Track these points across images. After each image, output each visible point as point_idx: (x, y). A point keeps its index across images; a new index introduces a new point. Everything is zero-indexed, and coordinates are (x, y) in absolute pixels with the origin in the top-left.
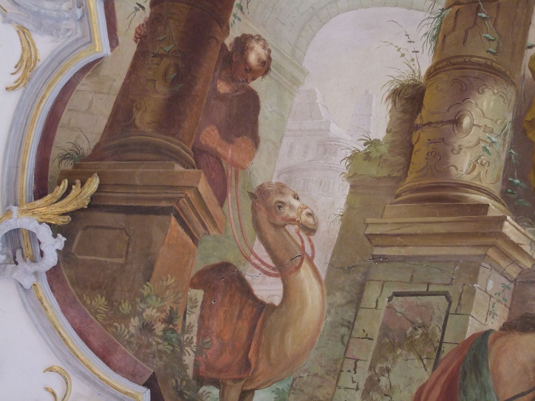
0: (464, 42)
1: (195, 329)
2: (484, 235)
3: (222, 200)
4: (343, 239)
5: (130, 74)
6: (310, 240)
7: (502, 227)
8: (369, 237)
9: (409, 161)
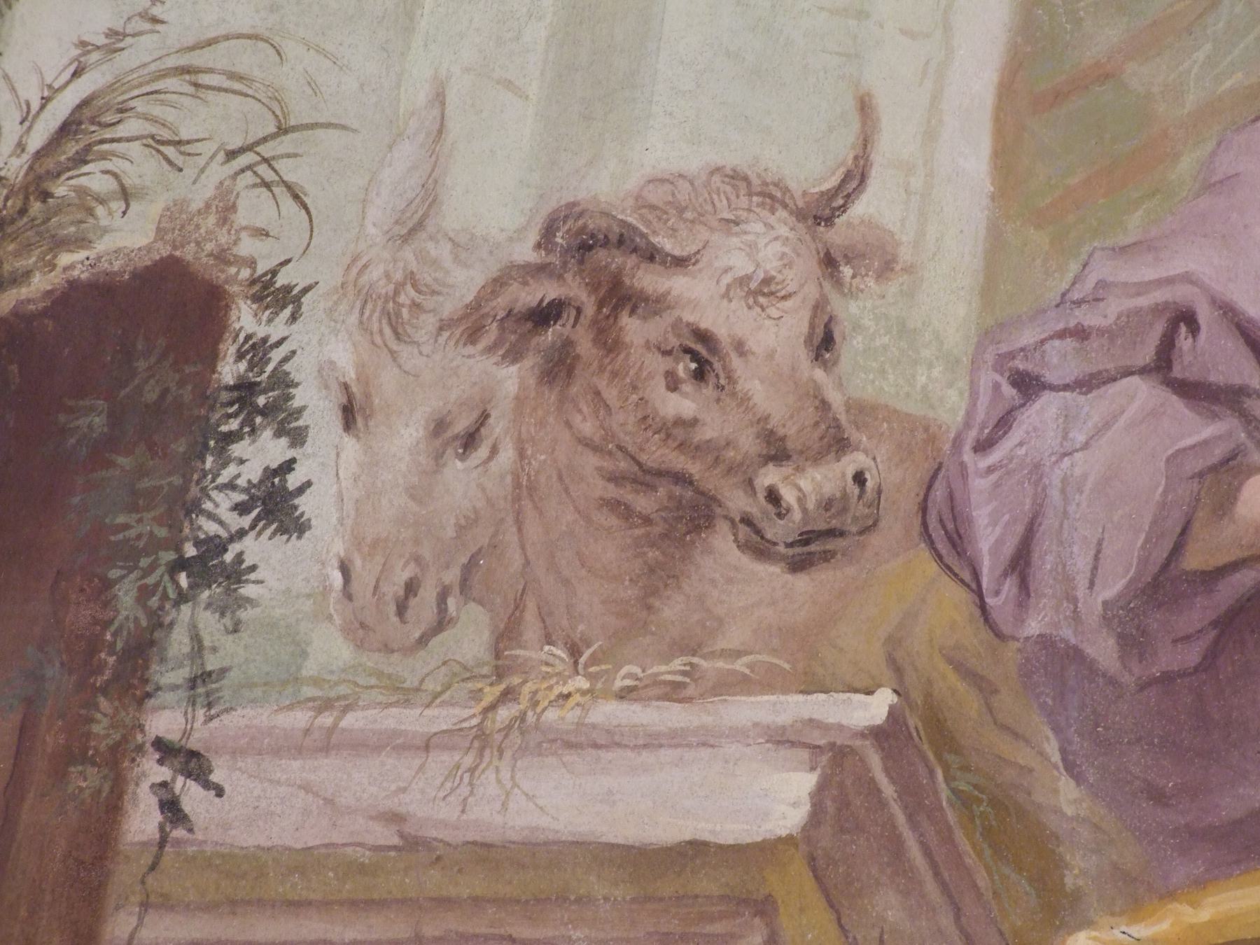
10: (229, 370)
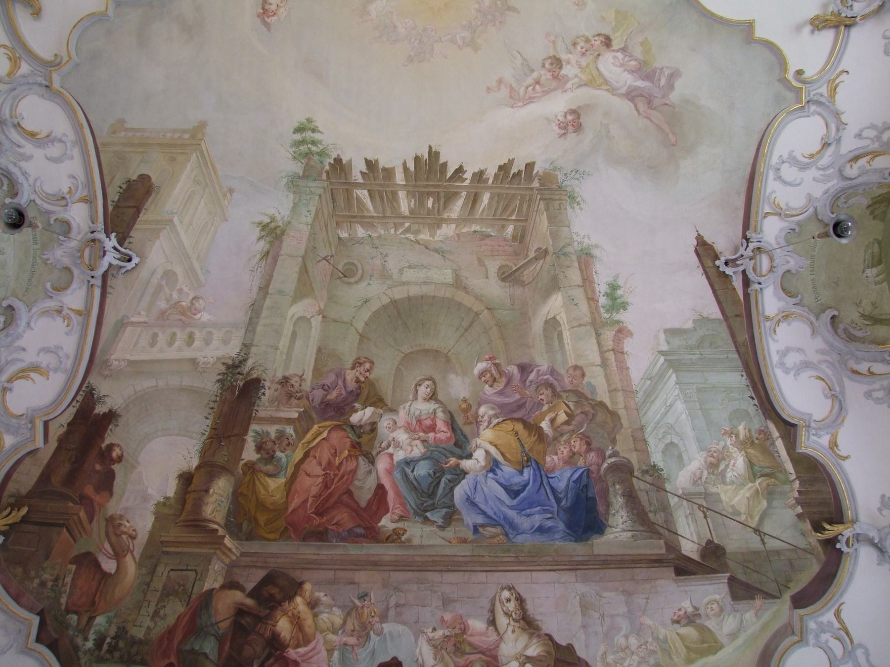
0: (214, 455)
3: (91, 521)
5: (51, 458)
6: (133, 543)
7: (224, 540)
8: (162, 542)
9: (183, 506)
10: (261, 385)
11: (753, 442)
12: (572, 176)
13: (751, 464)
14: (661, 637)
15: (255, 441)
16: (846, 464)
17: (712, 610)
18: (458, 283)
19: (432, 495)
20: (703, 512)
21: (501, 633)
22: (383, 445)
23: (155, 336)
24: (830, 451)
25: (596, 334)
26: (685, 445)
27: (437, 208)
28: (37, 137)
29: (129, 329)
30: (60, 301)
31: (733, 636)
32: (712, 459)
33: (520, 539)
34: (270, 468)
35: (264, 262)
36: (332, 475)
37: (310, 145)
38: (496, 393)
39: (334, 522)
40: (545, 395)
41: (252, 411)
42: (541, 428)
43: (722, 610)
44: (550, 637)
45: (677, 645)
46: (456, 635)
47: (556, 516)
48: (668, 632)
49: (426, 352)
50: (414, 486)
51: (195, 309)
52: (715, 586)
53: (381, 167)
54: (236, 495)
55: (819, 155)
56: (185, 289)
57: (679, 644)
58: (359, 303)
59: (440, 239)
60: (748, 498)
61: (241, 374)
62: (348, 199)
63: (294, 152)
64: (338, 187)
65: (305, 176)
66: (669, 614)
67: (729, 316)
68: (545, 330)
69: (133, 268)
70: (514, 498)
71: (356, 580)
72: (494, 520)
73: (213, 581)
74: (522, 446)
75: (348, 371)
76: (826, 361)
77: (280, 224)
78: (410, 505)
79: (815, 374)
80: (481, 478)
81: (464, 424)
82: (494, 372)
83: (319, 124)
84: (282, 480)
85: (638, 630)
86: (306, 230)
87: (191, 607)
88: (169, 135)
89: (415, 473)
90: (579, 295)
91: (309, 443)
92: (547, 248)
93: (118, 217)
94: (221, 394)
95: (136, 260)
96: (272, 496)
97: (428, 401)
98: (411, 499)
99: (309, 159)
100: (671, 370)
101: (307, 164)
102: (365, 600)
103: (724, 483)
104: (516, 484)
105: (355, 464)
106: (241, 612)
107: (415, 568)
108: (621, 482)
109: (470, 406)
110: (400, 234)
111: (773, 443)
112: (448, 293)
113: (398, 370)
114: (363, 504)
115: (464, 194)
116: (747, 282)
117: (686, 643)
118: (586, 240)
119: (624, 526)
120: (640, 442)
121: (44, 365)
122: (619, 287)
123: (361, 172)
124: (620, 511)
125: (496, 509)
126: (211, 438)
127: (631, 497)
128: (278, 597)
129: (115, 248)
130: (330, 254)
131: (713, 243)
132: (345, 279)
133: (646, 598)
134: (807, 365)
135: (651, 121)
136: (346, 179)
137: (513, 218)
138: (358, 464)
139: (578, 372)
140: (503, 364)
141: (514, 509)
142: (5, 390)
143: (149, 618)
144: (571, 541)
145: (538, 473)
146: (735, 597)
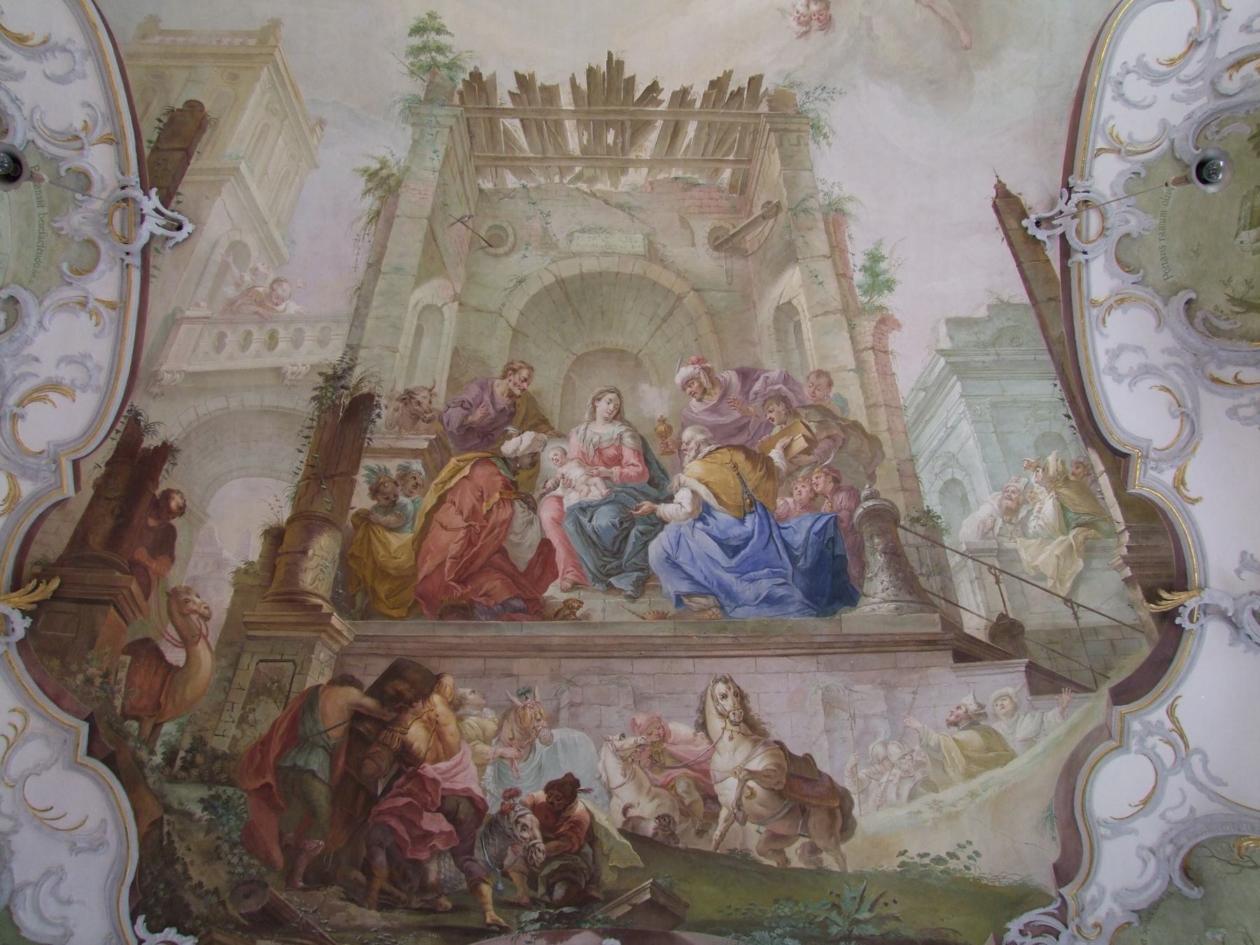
0: (312, 502)
1: (124, 682)
2: (320, 624)
3: (147, 596)
4: (228, 625)
5: (87, 510)
8: (245, 623)
11: (1067, 479)
12: (816, 95)
13: (1063, 509)
14: (932, 744)
15: (369, 482)
16: (1195, 510)
17: (1003, 708)
18: (653, 254)
19: (618, 553)
20: (995, 575)
21: (715, 741)
22: (549, 484)
23: (222, 336)
24: (1175, 491)
25: (849, 325)
26: (972, 483)
27: (620, 145)
28: (30, 43)
29: (184, 328)
30: (83, 289)
31: (1030, 742)
32: (1009, 502)
33: (740, 612)
34: (390, 519)
35: (373, 228)
36: (477, 527)
37: (434, 54)
38: (706, 410)
39: (482, 593)
40: (777, 411)
41: (364, 438)
42: (770, 459)
43: (1016, 708)
44: (781, 745)
45: (953, 754)
46: (653, 743)
47: (790, 582)
48: (944, 738)
49: (607, 352)
50: (592, 541)
51: (278, 297)
52: (1009, 676)
53: (538, 84)
54: (346, 559)
55: (1182, 61)
56: (262, 268)
57: (956, 753)
58: (513, 283)
59: (626, 189)
60: (1057, 556)
61: (347, 388)
62: (492, 132)
63: (412, 64)
64: (478, 115)
65: (429, 100)
66: (944, 714)
67: (1039, 299)
68: (776, 319)
69: (185, 240)
70: (732, 557)
71: (515, 672)
72: (705, 587)
73: (318, 674)
74: (743, 483)
75: (497, 382)
76: (1175, 365)
77: (395, 171)
78: (588, 567)
79: (1159, 382)
80: (686, 530)
81: (662, 454)
82: (703, 380)
83: (446, 21)
84: (408, 536)
85: (901, 736)
86: (432, 178)
87: (291, 710)
88: (226, 41)
89: (594, 523)
90: (825, 269)
91: (444, 482)
92: (779, 202)
93: (159, 164)
94: (319, 417)
95: (188, 228)
96: (396, 558)
97: (611, 422)
98: (589, 560)
99: (434, 74)
100: (955, 377)
101: (431, 82)
102: (527, 698)
103: (1025, 535)
104: (735, 537)
105: (509, 511)
106: (357, 715)
107: (595, 654)
108: (882, 533)
109: (670, 428)
110: (568, 183)
111: (1095, 481)
112: (637, 268)
113: (568, 378)
114: (522, 567)
115: (659, 123)
116: (1066, 251)
117: (965, 752)
118: (836, 190)
119: (884, 595)
120: (908, 477)
121: (67, 381)
122: (882, 258)
123: (510, 92)
124: (880, 574)
125: (706, 573)
126: (308, 478)
127: (895, 555)
128: (409, 695)
129: (157, 210)
130: (468, 214)
131: (1020, 194)
132: (491, 250)
133: (914, 693)
134: (1147, 370)
135: (934, 11)
136: (488, 103)
137: (731, 157)
138: (513, 513)
139: (823, 380)
140: (716, 369)
141: (731, 572)
142: (15, 417)
143: (234, 726)
144: (811, 615)
145: (765, 521)
146: (1035, 690)
